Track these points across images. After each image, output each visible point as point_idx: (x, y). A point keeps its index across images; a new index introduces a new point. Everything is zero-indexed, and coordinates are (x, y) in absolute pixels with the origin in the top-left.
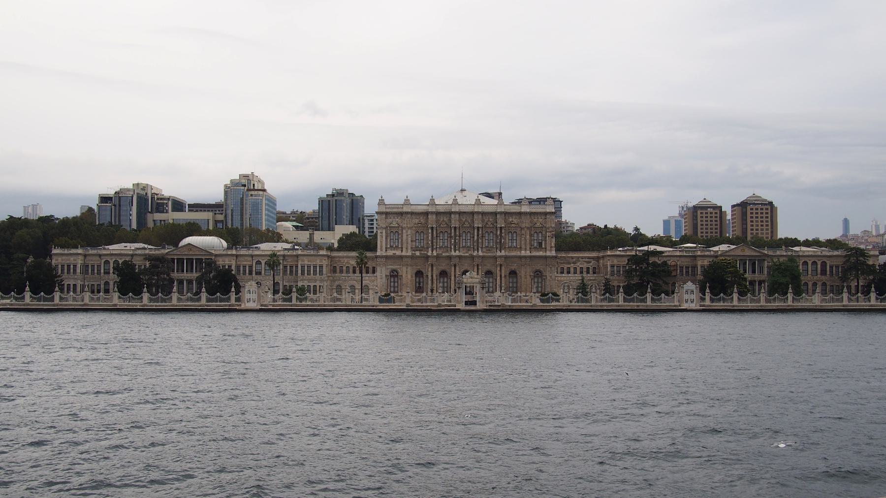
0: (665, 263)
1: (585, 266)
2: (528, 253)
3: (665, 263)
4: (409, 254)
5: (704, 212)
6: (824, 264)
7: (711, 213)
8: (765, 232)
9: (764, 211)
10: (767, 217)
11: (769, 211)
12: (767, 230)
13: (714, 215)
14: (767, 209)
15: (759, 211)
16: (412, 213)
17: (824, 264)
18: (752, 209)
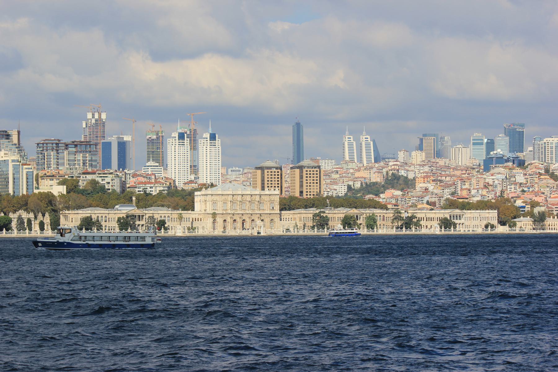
0: (326, 216)
1: (287, 217)
2: (269, 212)
3: (326, 216)
4: (221, 212)
5: (270, 171)
6: (384, 216)
7: (275, 172)
8: (315, 187)
9: (315, 173)
10: (317, 177)
11: (318, 173)
12: (317, 186)
13: (276, 174)
14: (317, 171)
15: (312, 173)
16: (222, 195)
17: (384, 216)
18: (307, 171)
